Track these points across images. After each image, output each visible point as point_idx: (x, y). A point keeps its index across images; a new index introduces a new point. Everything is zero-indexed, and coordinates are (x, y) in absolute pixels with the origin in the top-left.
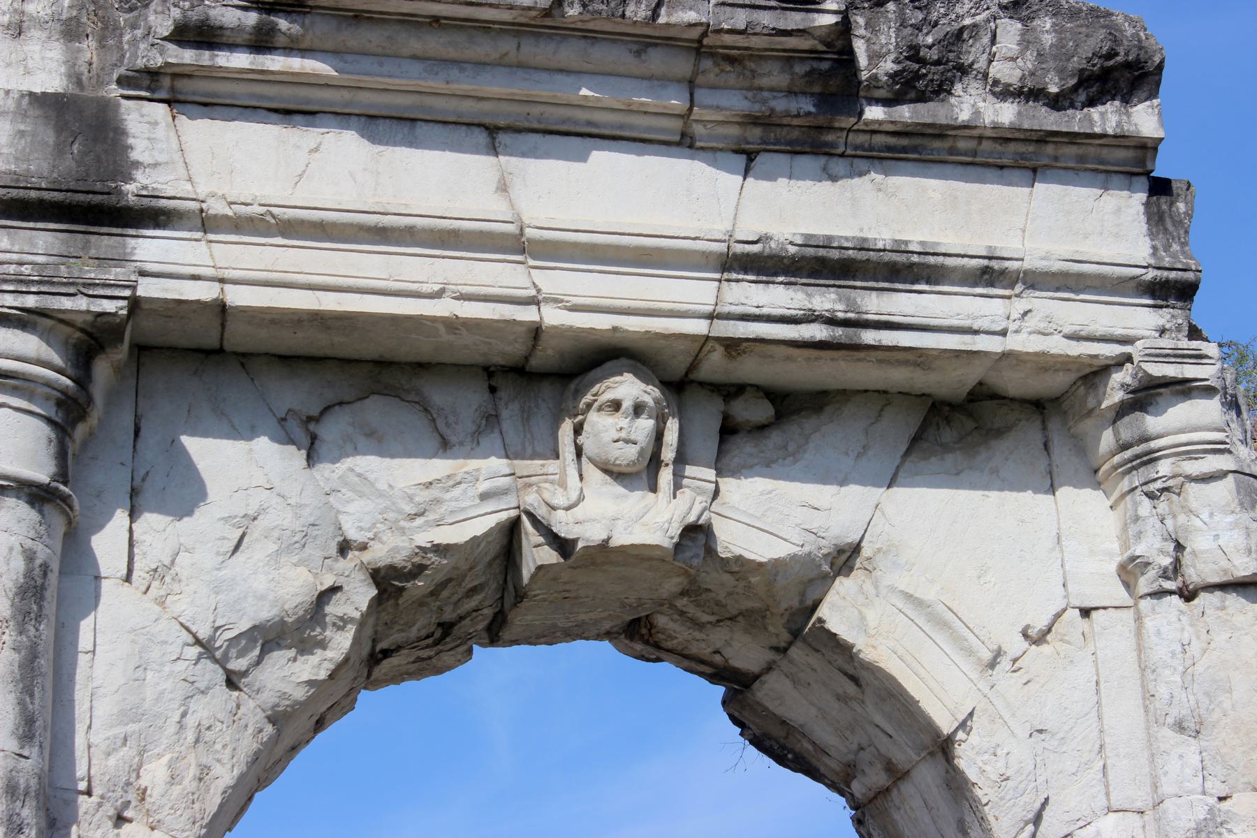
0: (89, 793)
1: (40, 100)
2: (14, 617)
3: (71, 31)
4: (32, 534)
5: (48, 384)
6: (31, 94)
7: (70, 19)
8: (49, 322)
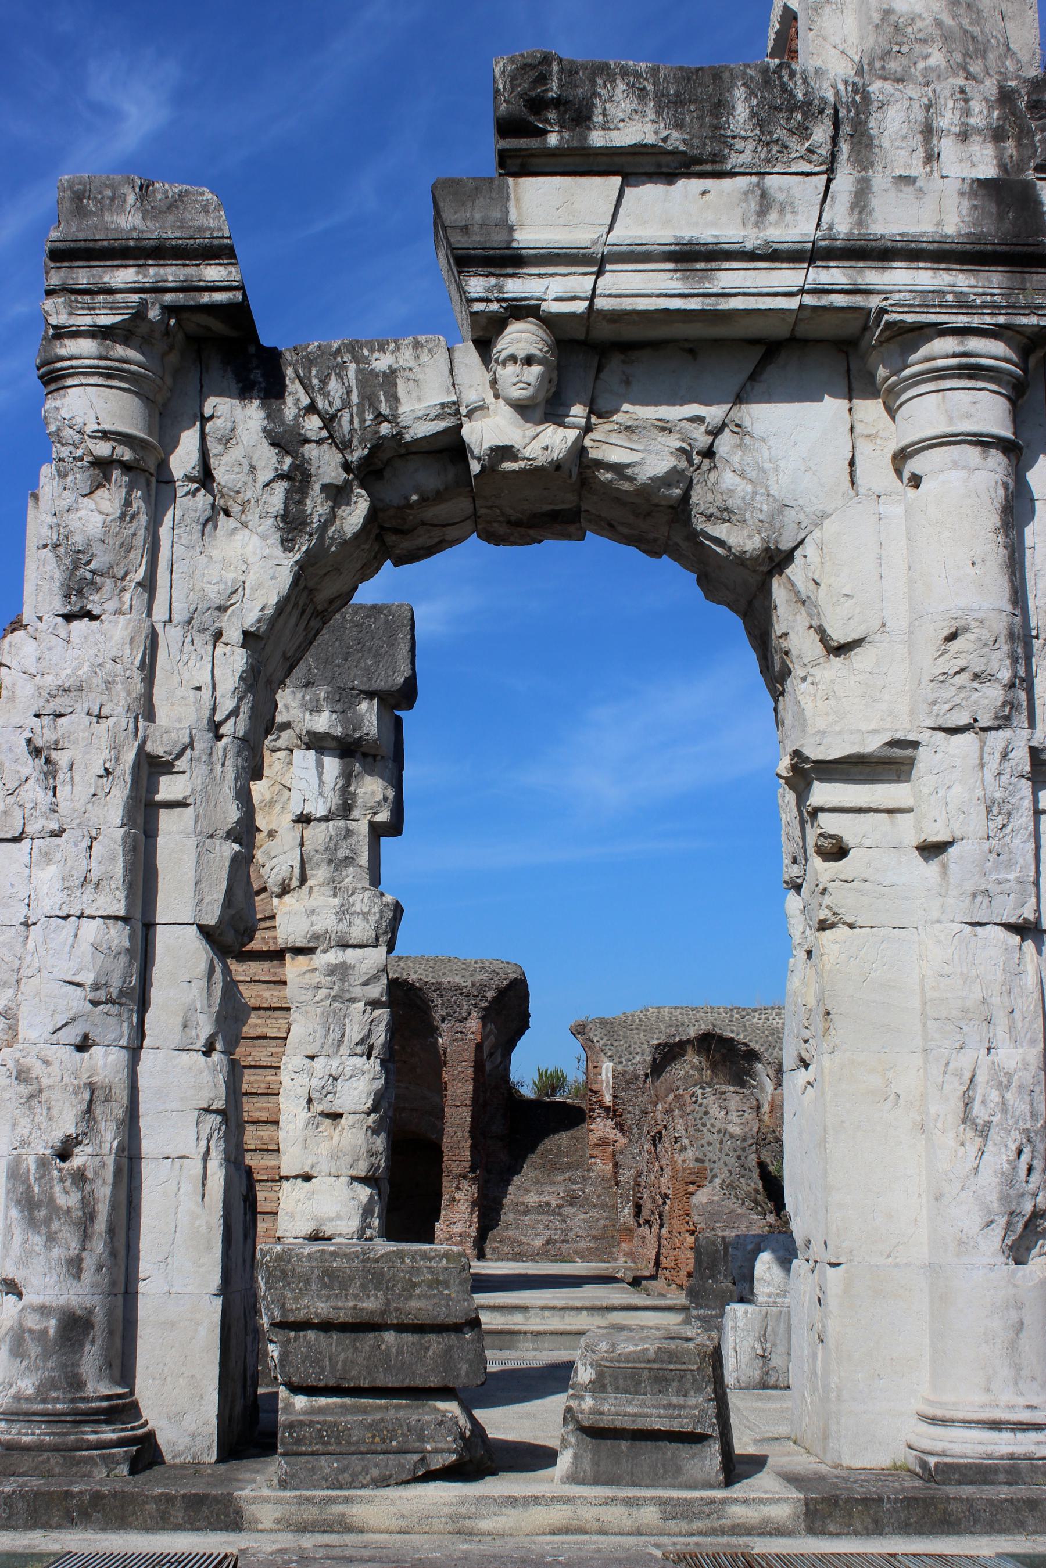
0: (1037, 637)
1: (984, 184)
2: (1002, 526)
3: (998, 136)
4: (1006, 473)
5: (1010, 374)
6: (978, 180)
7: (998, 127)
8: (1010, 333)
